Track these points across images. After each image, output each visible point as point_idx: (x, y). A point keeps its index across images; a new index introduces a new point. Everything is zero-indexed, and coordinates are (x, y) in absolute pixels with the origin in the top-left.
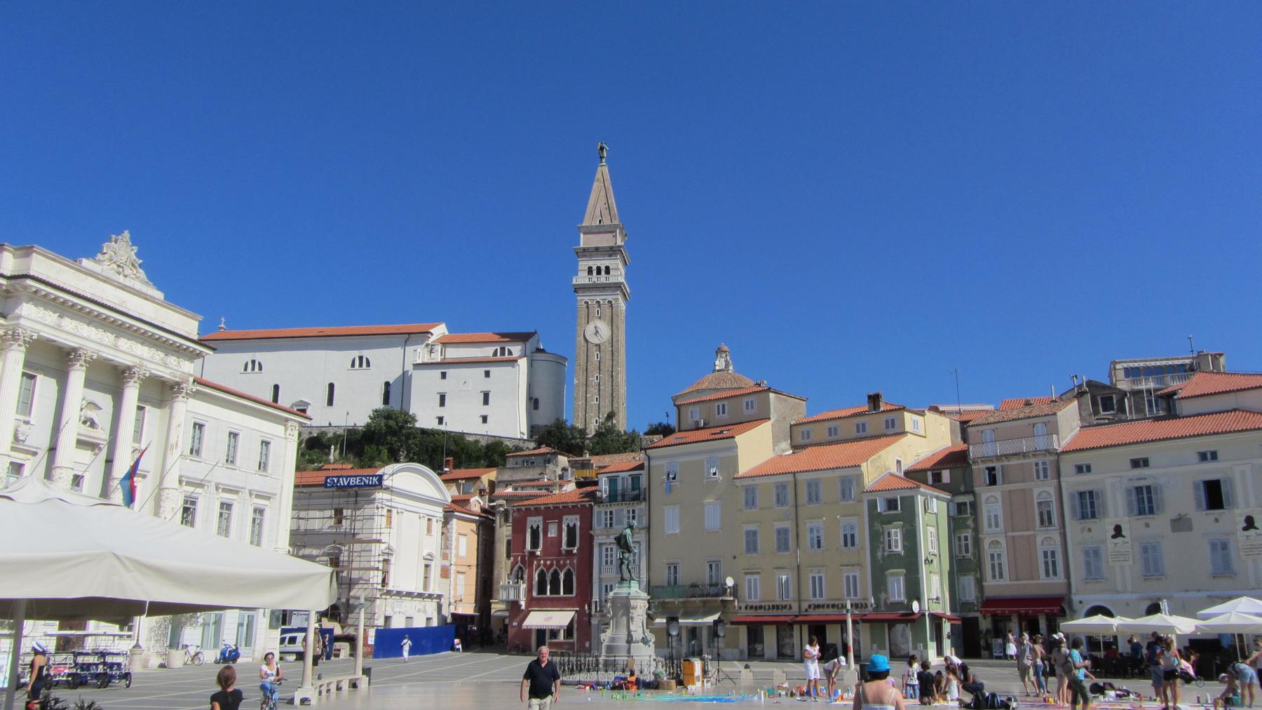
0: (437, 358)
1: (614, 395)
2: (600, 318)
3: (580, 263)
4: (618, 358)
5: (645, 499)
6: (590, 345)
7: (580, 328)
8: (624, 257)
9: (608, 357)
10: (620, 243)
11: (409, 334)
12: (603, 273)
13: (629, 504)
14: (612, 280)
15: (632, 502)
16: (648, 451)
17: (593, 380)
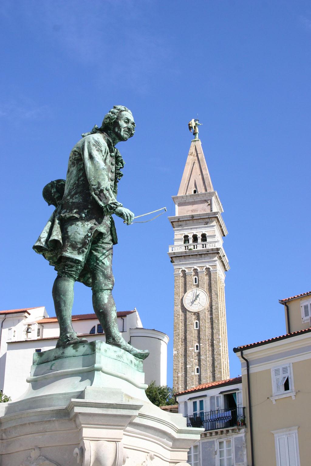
0: (33, 336)
1: (216, 364)
2: (198, 286)
3: (176, 233)
4: (218, 325)
5: (244, 424)
6: (188, 315)
7: (177, 297)
8: (221, 227)
9: (208, 325)
10: (215, 209)
11: (6, 314)
12: (199, 240)
13: (222, 432)
14: (209, 247)
15: (225, 430)
16: (245, 352)
17: (192, 349)
